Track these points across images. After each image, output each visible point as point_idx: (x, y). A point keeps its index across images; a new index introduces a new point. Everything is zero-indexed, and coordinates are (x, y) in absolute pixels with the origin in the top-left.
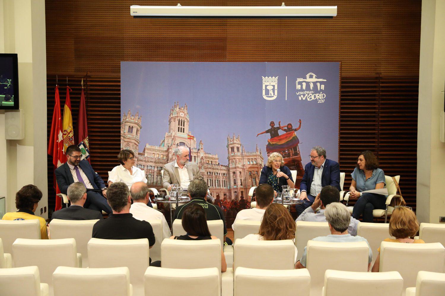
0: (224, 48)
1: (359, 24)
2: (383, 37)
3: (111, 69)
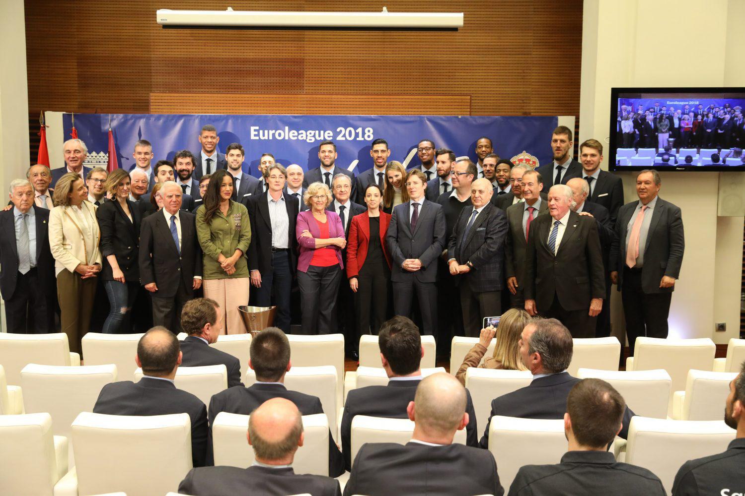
0: (300, 75)
1: (498, 41)
2: (534, 59)
3: (132, 104)
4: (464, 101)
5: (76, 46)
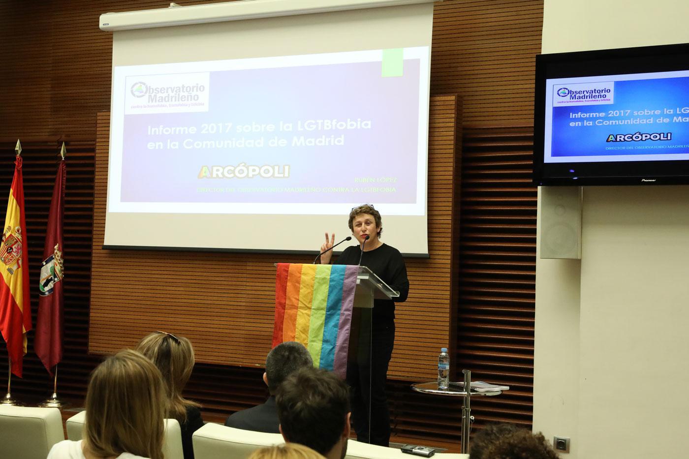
1: (517, 17)
4: (447, 103)
5: (51, 65)
